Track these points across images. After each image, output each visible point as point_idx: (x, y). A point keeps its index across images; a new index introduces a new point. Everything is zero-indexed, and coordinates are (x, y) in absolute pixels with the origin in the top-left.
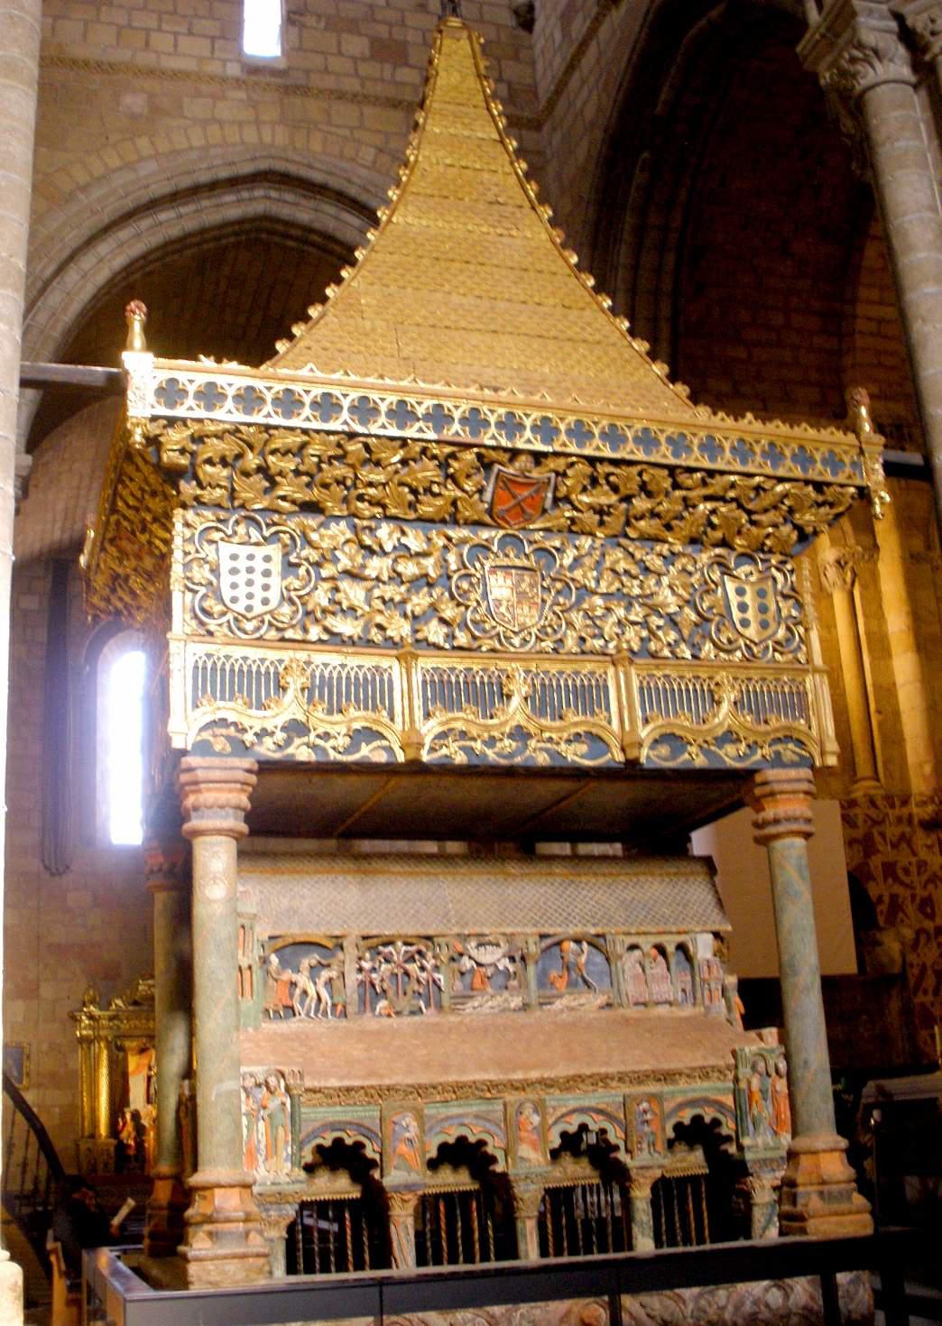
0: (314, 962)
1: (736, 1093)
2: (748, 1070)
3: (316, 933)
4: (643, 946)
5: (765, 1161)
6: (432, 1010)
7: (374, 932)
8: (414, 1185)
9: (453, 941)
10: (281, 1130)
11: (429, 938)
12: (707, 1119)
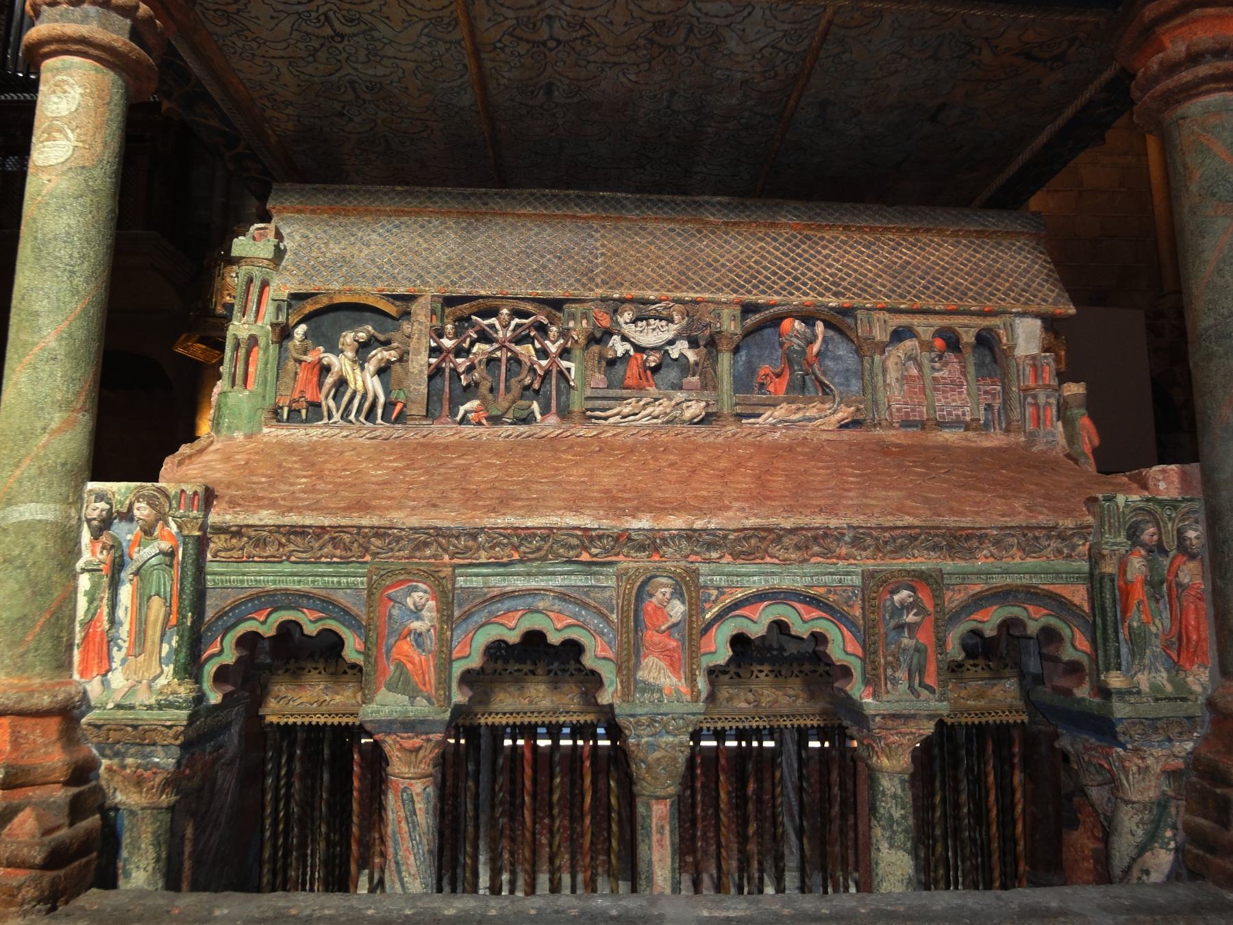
0: (362, 336)
1: (1095, 581)
2: (1122, 538)
3: (368, 291)
4: (920, 329)
6: (553, 419)
10: (156, 603)
11: (557, 304)
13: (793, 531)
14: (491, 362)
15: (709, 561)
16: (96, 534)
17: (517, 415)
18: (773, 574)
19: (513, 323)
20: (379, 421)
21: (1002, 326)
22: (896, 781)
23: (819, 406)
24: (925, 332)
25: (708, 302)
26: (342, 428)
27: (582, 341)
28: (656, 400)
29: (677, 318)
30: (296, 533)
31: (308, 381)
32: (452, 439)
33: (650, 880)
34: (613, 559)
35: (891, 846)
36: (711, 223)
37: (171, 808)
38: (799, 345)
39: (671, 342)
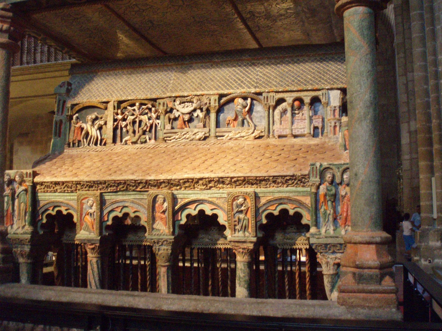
0: (94, 117)
4: (287, 99)
5: (326, 245)
6: (153, 141)
7: (123, 99)
8: (93, 240)
9: (167, 101)
11: (155, 100)
12: (291, 212)
13: (201, 179)
14: (134, 122)
15: (177, 190)
16: (8, 186)
17: (142, 141)
18: (198, 194)
19: (141, 108)
20: (99, 145)
21: (321, 94)
22: (242, 264)
23: (246, 131)
24: (289, 100)
25: (207, 95)
26: (88, 148)
27: (164, 113)
28: (188, 132)
29: (195, 101)
30: (57, 184)
31: (77, 133)
32: (120, 150)
33: (161, 291)
34: (147, 190)
35: (240, 286)
36: (216, 62)
37: (30, 263)
38: (240, 109)
39: (195, 110)
